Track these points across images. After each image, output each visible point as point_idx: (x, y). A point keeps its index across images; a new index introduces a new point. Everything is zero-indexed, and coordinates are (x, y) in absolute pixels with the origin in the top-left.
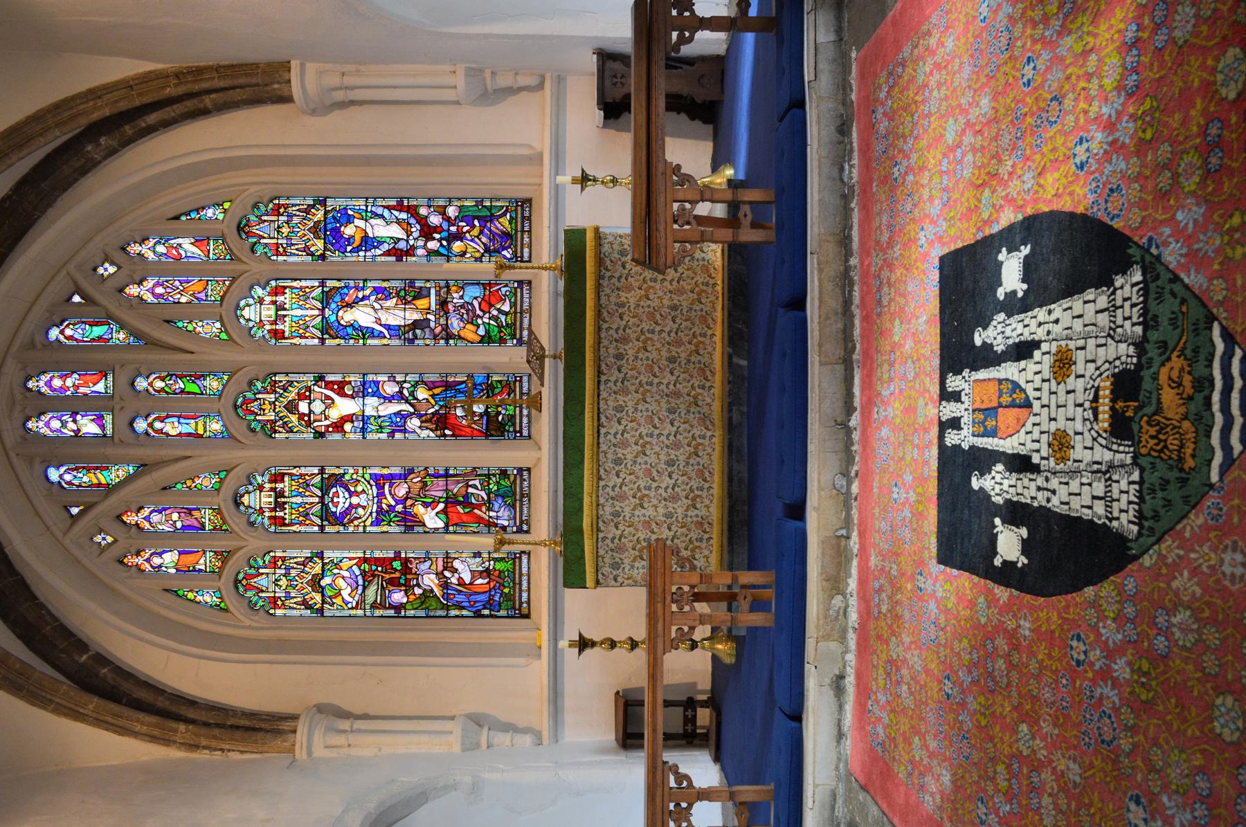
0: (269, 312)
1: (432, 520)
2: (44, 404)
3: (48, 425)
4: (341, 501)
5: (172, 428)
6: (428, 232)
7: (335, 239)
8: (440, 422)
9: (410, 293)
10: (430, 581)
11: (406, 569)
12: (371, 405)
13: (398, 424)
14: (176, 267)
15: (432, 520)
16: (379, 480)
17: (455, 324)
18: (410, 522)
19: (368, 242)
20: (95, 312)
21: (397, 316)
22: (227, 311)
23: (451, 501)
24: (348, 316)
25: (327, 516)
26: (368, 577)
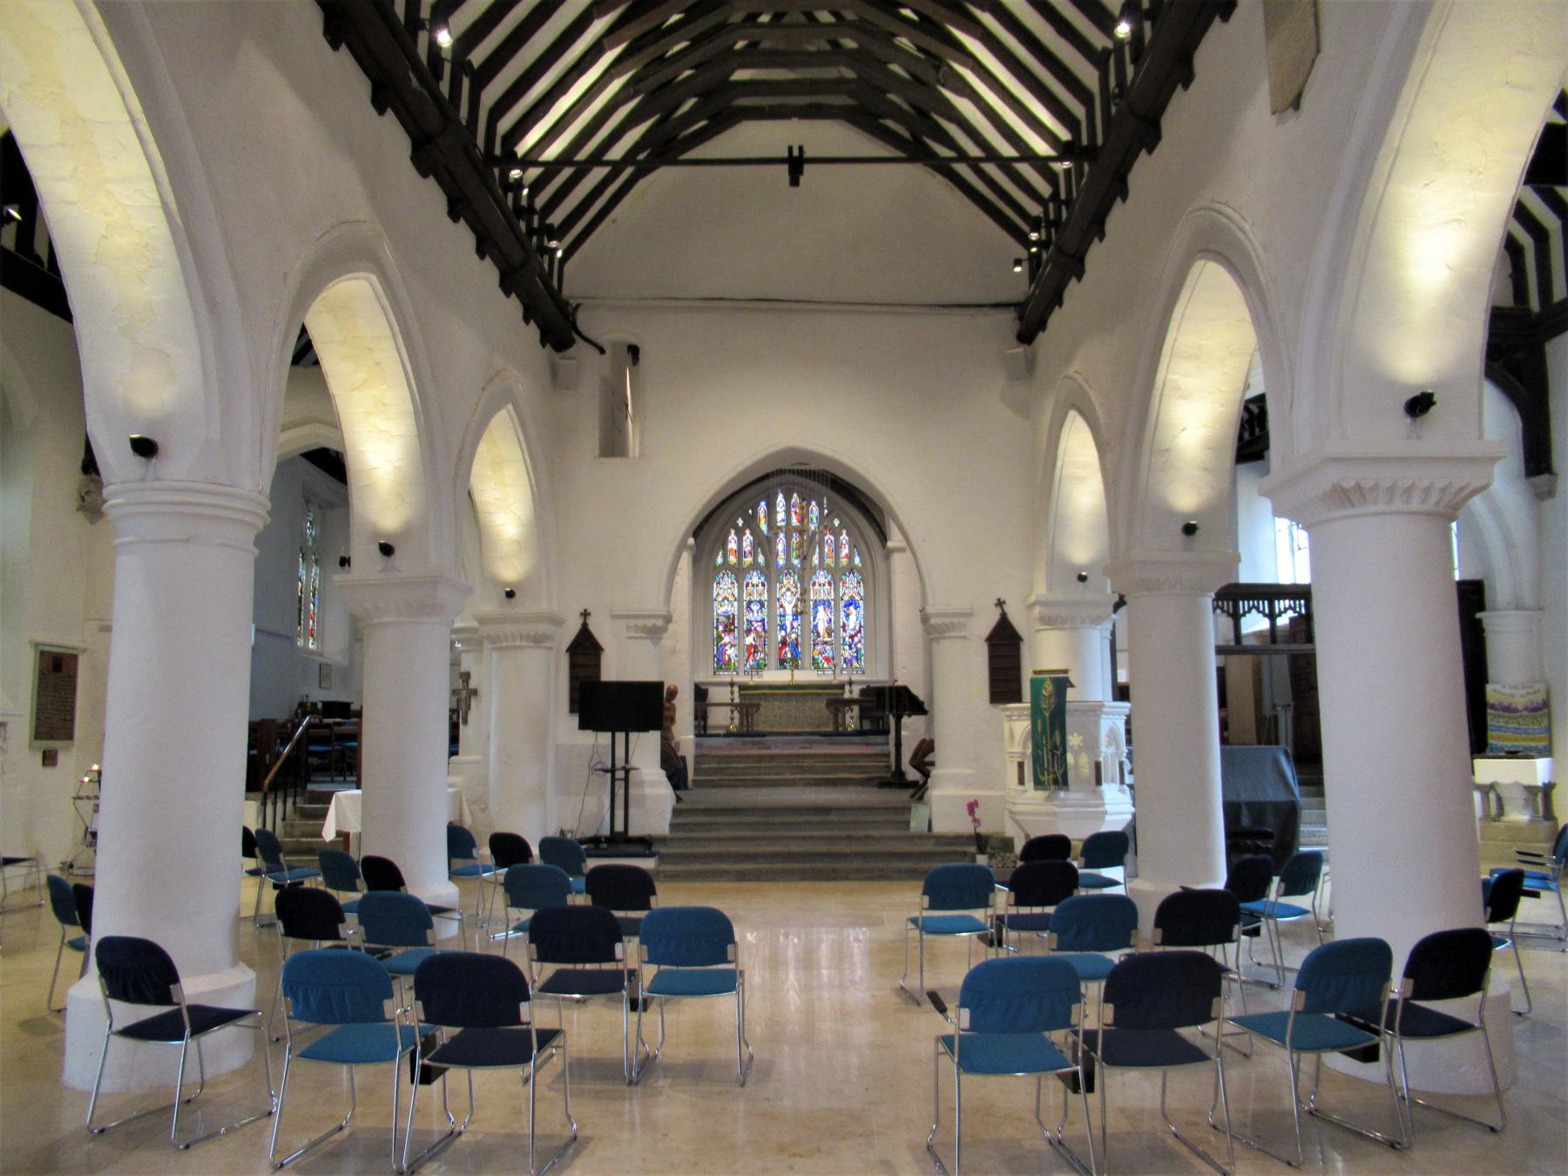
0: (822, 580)
1: (749, 640)
2: (788, 498)
3: (780, 498)
4: (755, 607)
5: (780, 547)
6: (852, 637)
7: (848, 605)
8: (784, 643)
9: (829, 632)
10: (727, 639)
11: (731, 631)
12: (789, 618)
13: (783, 627)
14: (837, 547)
15: (749, 640)
16: (763, 621)
17: (819, 647)
18: (749, 631)
19: (848, 616)
20: (821, 518)
21: (821, 629)
22: (822, 566)
23: (755, 647)
24: (821, 608)
25: (750, 602)
26: (728, 617)
